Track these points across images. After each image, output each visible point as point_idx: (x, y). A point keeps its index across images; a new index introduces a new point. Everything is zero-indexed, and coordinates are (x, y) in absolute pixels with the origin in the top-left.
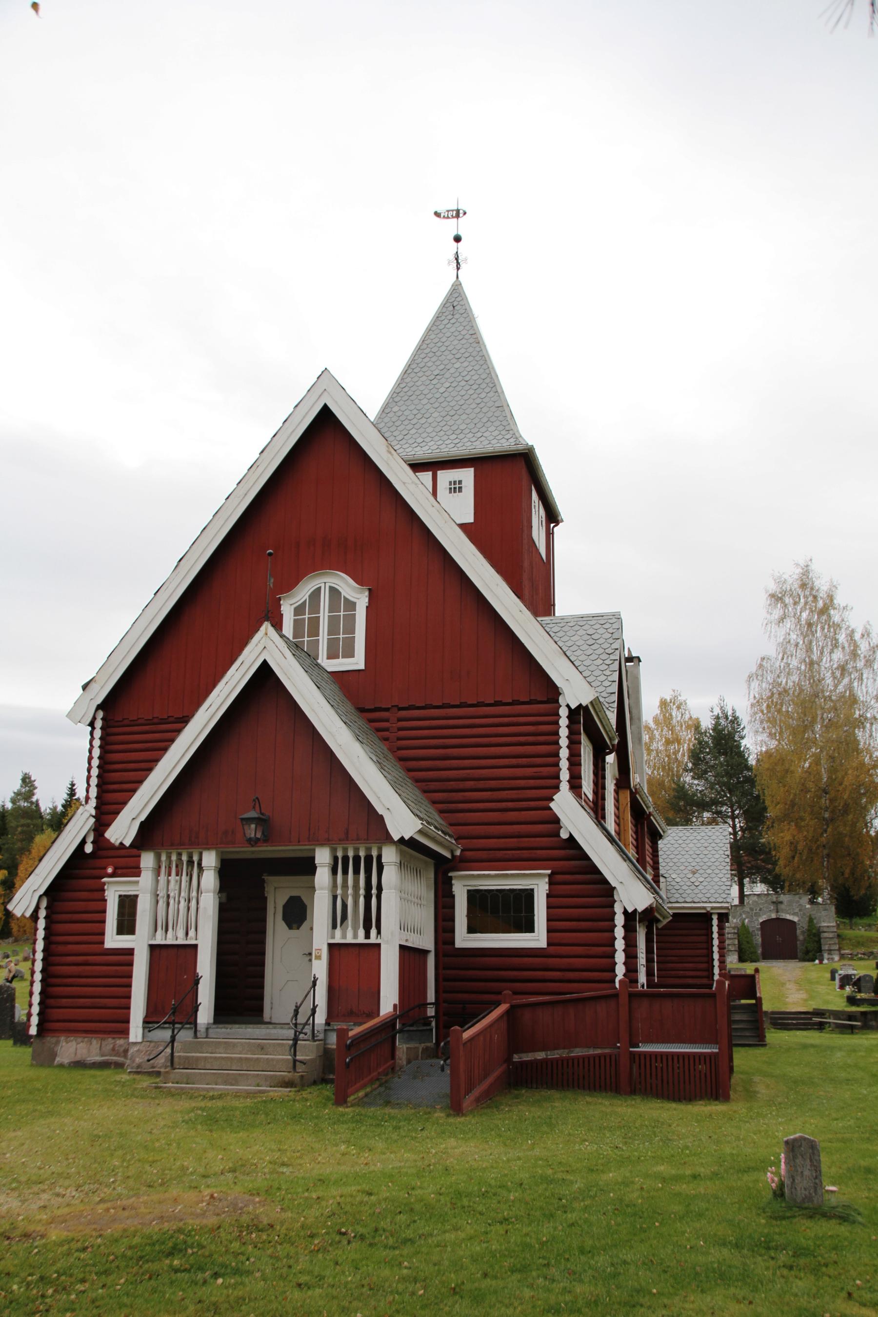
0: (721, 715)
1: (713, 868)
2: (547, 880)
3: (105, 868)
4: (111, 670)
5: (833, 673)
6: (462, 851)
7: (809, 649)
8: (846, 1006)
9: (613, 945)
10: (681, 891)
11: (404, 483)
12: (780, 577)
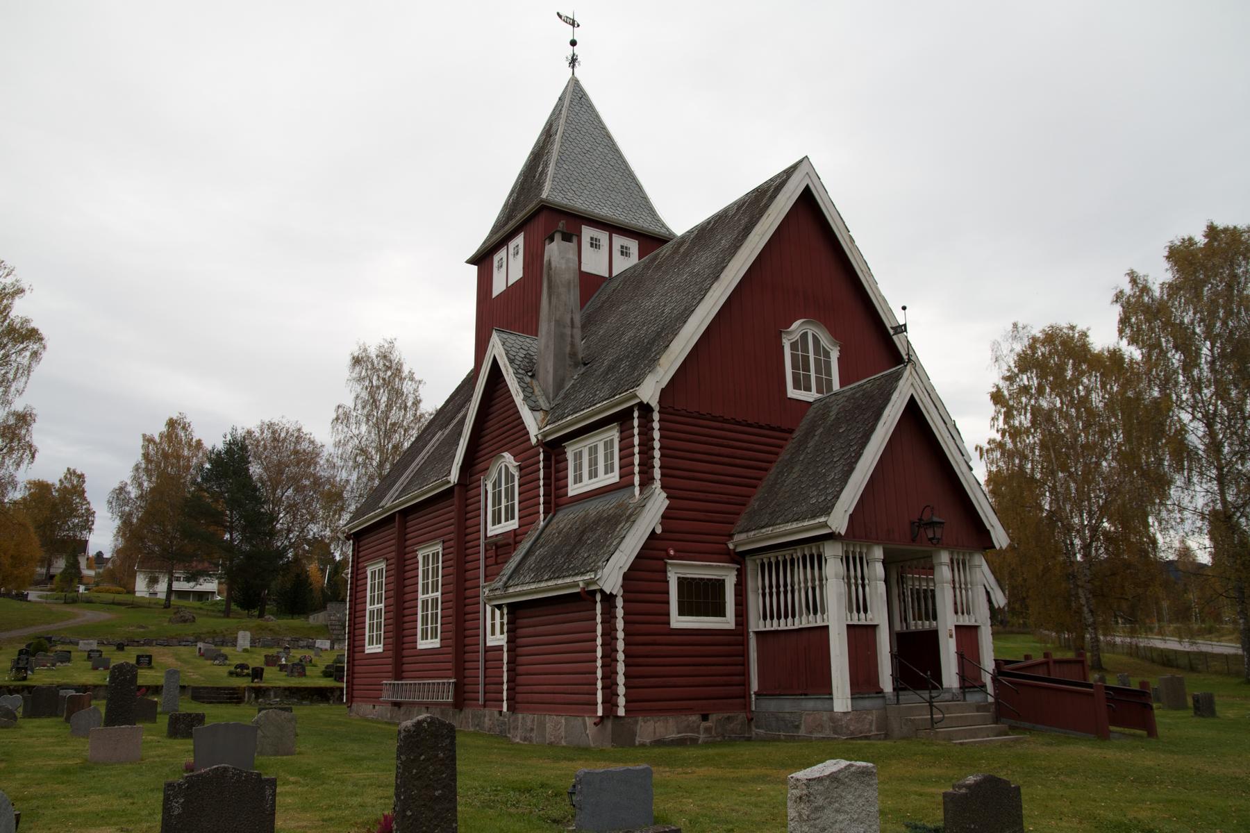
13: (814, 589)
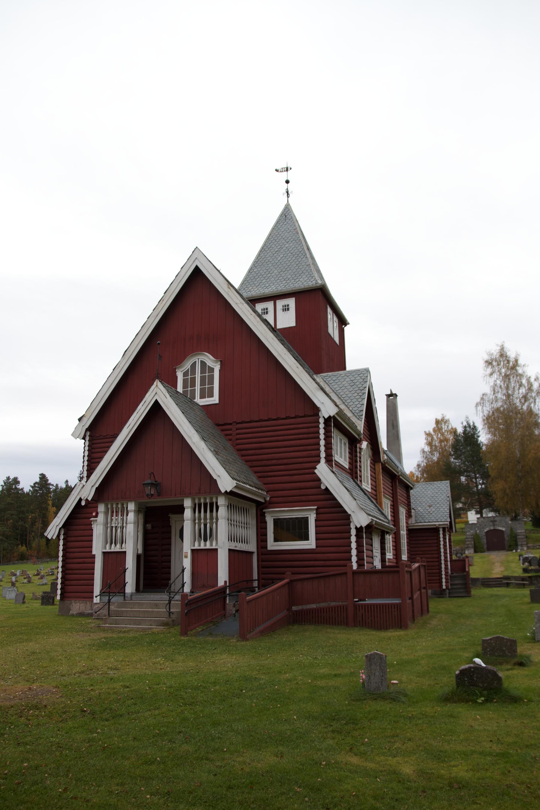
0: (467, 426)
1: (440, 503)
2: (315, 512)
3: (92, 513)
4: (92, 410)
5: (520, 400)
6: (270, 498)
7: (507, 388)
8: (522, 574)
9: (350, 546)
10: (423, 517)
11: (237, 303)
12: (489, 352)
13: (205, 525)
